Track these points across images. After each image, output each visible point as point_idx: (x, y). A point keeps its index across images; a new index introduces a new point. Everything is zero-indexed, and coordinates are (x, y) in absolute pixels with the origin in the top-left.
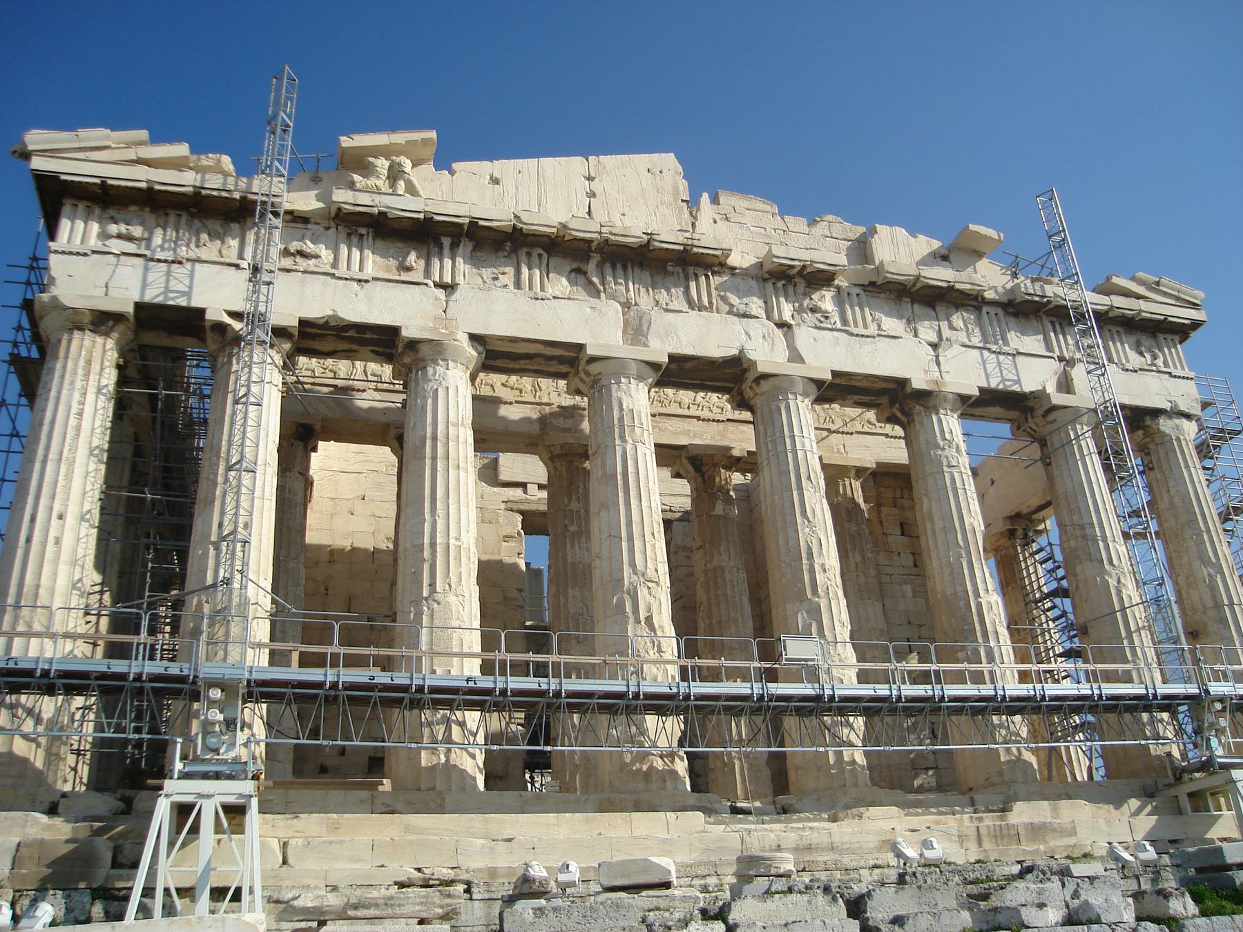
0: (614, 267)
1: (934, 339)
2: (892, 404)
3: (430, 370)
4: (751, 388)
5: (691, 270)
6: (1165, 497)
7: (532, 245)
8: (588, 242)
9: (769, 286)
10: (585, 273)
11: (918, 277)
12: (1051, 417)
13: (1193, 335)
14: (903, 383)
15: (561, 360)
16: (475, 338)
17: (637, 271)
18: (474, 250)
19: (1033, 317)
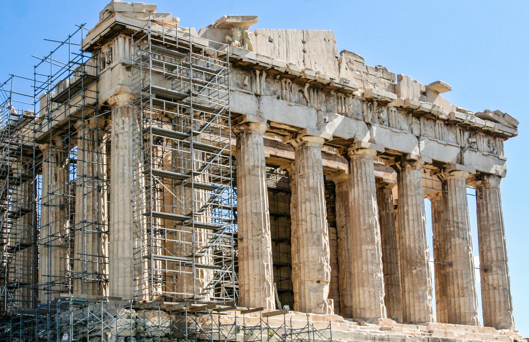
0: (314, 91)
1: (418, 135)
2: (396, 160)
3: (253, 135)
4: (353, 151)
5: (340, 94)
6: (485, 212)
7: (287, 78)
8: (309, 80)
9: (365, 106)
10: (303, 92)
11: (419, 108)
12: (452, 174)
13: (510, 139)
14: (405, 155)
15: (290, 131)
16: (269, 122)
17: (320, 93)
18: (266, 78)
19: (453, 126)
